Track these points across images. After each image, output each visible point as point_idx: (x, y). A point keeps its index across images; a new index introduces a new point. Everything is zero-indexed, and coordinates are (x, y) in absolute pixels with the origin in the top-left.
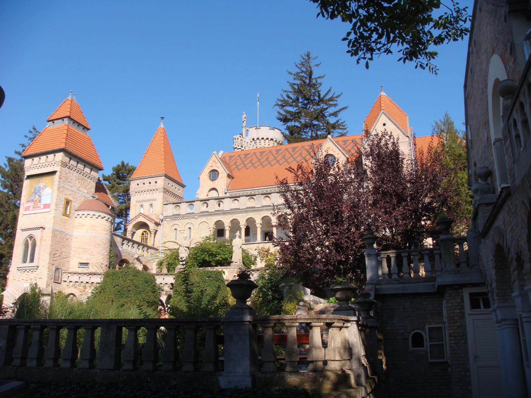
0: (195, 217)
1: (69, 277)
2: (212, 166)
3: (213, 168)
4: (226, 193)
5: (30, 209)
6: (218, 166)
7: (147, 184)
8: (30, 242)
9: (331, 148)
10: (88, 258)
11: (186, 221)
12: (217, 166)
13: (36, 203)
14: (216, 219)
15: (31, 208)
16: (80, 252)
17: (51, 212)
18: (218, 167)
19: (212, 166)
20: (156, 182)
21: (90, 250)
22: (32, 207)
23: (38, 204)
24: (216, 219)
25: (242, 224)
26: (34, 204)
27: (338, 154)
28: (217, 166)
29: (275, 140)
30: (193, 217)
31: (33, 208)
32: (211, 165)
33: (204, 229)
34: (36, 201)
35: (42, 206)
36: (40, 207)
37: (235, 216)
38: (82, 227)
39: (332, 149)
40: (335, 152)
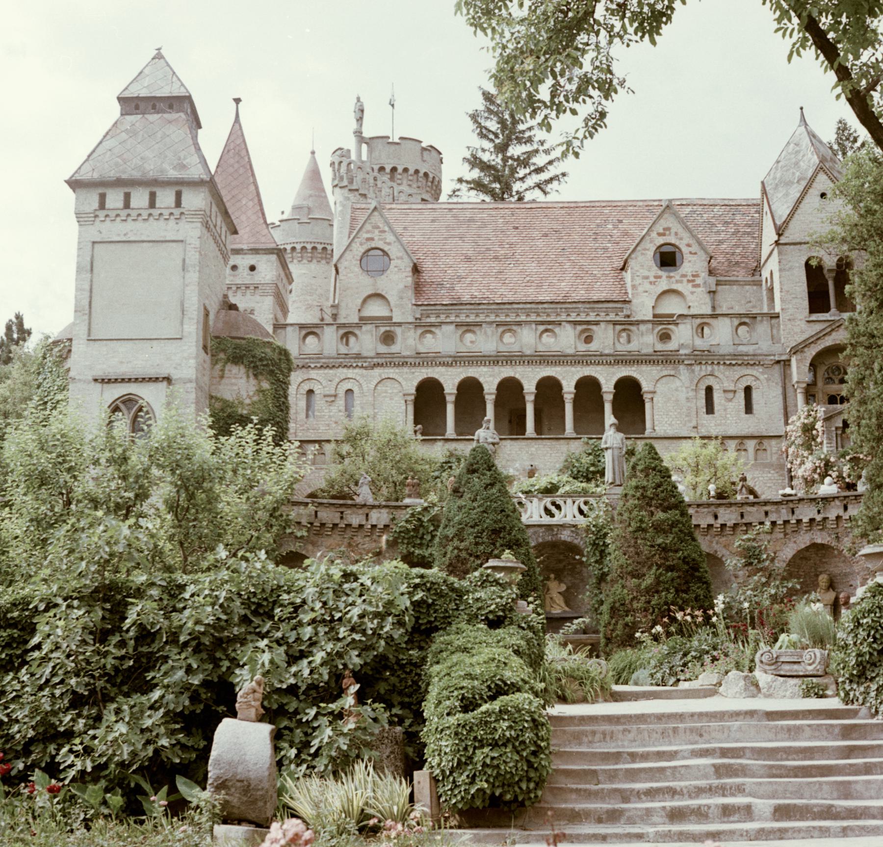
2: (372, 239)
7: (243, 271)
9: (673, 231)
11: (343, 372)
18: (389, 244)
19: (372, 239)
20: (252, 268)
27: (689, 245)
28: (385, 239)
29: (431, 176)
32: (369, 236)
37: (472, 372)
38: (233, 381)
40: (681, 239)
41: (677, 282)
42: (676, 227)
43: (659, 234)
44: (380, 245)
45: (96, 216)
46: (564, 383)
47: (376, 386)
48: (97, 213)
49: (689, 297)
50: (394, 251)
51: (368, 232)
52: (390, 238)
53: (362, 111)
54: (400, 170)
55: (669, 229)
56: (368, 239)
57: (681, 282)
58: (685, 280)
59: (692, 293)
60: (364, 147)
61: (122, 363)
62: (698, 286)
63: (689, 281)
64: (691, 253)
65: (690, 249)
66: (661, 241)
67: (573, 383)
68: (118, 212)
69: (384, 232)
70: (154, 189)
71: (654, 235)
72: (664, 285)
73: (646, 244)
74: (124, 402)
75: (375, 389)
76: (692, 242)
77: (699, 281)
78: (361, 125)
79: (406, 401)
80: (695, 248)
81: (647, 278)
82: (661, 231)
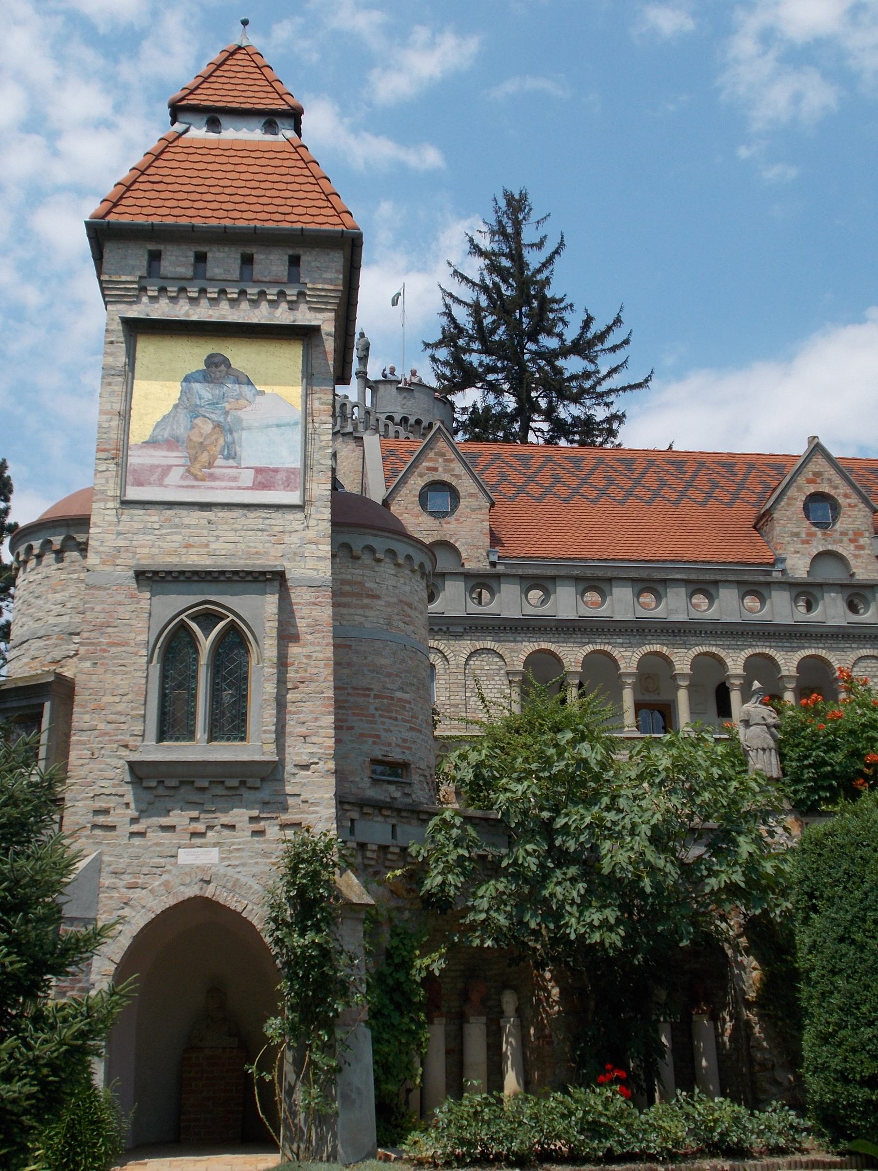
0: (452, 629)
1: (352, 821)
2: (435, 469)
3: (436, 477)
4: (493, 564)
5: (167, 481)
6: (456, 472)
8: (206, 643)
9: (826, 475)
10: (405, 741)
12: (453, 470)
13: (204, 457)
14: (528, 647)
15: (175, 476)
16: (373, 711)
17: (311, 510)
18: (458, 477)
19: (435, 469)
21: (407, 705)
22: (182, 470)
23: (219, 462)
24: (528, 647)
25: (630, 670)
26: (194, 459)
27: (846, 496)
28: (453, 470)
30: (444, 629)
31: (189, 472)
32: (431, 464)
33: (486, 675)
34: (202, 447)
35: (247, 478)
36: (234, 479)
38: (366, 601)
39: (829, 479)
41: (835, 542)
42: (830, 473)
43: (809, 481)
44: (446, 477)
45: (143, 289)
46: (729, 662)
47: (467, 660)
48: (144, 283)
49: (852, 562)
50: (466, 485)
51: (431, 460)
52: (459, 468)
53: (367, 349)
54: (412, 421)
55: (817, 474)
56: (429, 469)
57: (841, 541)
58: (845, 539)
59: (856, 556)
60: (368, 392)
61: (188, 546)
62: (861, 548)
63: (851, 541)
64: (850, 506)
65: (848, 500)
66: (811, 489)
67: (741, 662)
68: (184, 284)
69: (452, 461)
70: (248, 250)
71: (801, 480)
72: (817, 547)
73: (792, 492)
74: (193, 618)
75: (466, 664)
76: (849, 491)
77: (862, 541)
78: (365, 365)
79: (510, 682)
80: (854, 499)
81: (797, 535)
82: (810, 476)
